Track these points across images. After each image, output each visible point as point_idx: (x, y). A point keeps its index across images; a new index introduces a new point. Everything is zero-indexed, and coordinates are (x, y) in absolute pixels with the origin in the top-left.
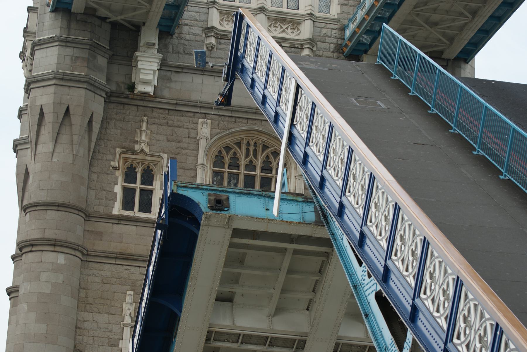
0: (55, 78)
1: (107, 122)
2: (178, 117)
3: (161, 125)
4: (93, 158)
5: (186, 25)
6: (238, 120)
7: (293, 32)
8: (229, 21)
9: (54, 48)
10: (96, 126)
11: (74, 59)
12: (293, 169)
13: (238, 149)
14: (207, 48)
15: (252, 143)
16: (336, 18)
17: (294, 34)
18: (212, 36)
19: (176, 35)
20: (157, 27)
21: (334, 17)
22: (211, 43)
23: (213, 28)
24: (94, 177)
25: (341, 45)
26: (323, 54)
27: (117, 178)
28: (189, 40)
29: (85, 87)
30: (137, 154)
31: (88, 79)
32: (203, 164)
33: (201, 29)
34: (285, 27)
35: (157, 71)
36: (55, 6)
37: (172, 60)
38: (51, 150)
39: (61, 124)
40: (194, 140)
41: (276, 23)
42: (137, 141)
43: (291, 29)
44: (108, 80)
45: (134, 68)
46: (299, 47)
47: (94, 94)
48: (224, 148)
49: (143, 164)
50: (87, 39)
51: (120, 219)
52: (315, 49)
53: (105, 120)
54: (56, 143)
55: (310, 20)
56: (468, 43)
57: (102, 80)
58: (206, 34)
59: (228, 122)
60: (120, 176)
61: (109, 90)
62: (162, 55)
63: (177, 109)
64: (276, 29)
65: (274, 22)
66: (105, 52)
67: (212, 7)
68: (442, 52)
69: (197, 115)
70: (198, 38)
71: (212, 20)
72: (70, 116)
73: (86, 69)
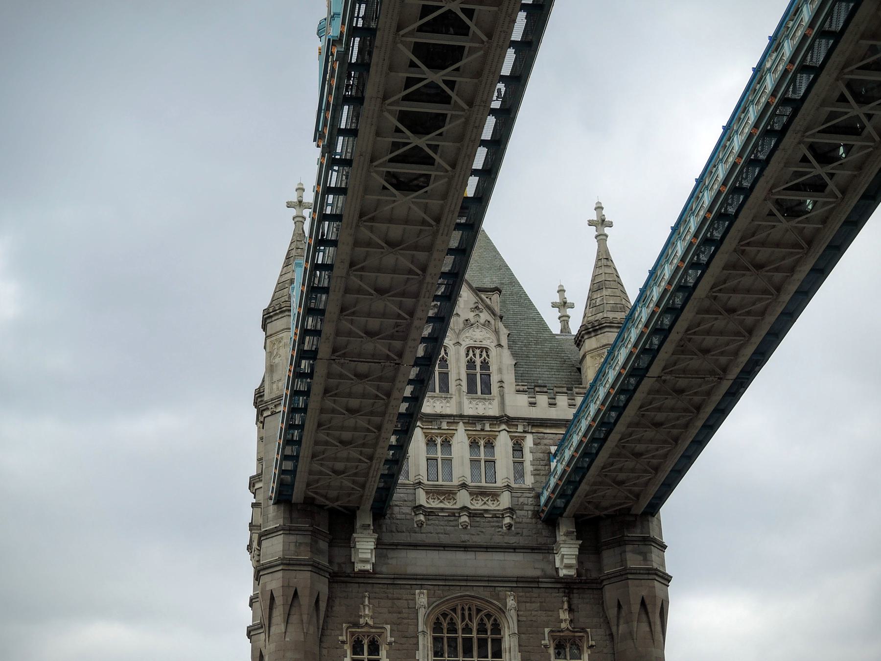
0: (282, 564)
1: (332, 600)
2: (396, 590)
3: (381, 599)
4: (322, 635)
5: (397, 506)
6: (452, 588)
7: (493, 504)
8: (434, 499)
9: (278, 537)
10: (323, 605)
11: (298, 545)
12: (506, 628)
13: (454, 615)
14: (417, 525)
15: (466, 608)
16: (531, 487)
17: (495, 505)
18: (421, 513)
19: (388, 515)
20: (370, 511)
21: (529, 487)
22: (420, 520)
23: (421, 506)
24: (325, 652)
25: (538, 511)
26: (522, 521)
27: (346, 651)
28: (400, 519)
29: (310, 569)
30: (362, 627)
31: (312, 562)
32: (423, 631)
33: (410, 508)
34: (485, 500)
35: (374, 550)
36: (277, 499)
37: (387, 538)
38: (283, 631)
39: (291, 605)
40: (414, 610)
41: (476, 497)
42: (361, 615)
43: (491, 501)
44: (330, 562)
45: (352, 549)
46: (501, 516)
47: (318, 575)
48: (441, 615)
49: (368, 636)
50: (308, 526)
52: (514, 517)
53: (331, 600)
54: (287, 623)
55: (507, 491)
56: (653, 498)
57: (324, 561)
58: (415, 512)
59: (443, 590)
60: (348, 648)
61: (331, 571)
62: (377, 535)
63: (395, 582)
64: (478, 502)
65: (475, 496)
66: (325, 537)
67: (418, 488)
68: (629, 509)
69: (413, 586)
70: (408, 517)
71: (419, 499)
72: (298, 598)
73: (310, 553)
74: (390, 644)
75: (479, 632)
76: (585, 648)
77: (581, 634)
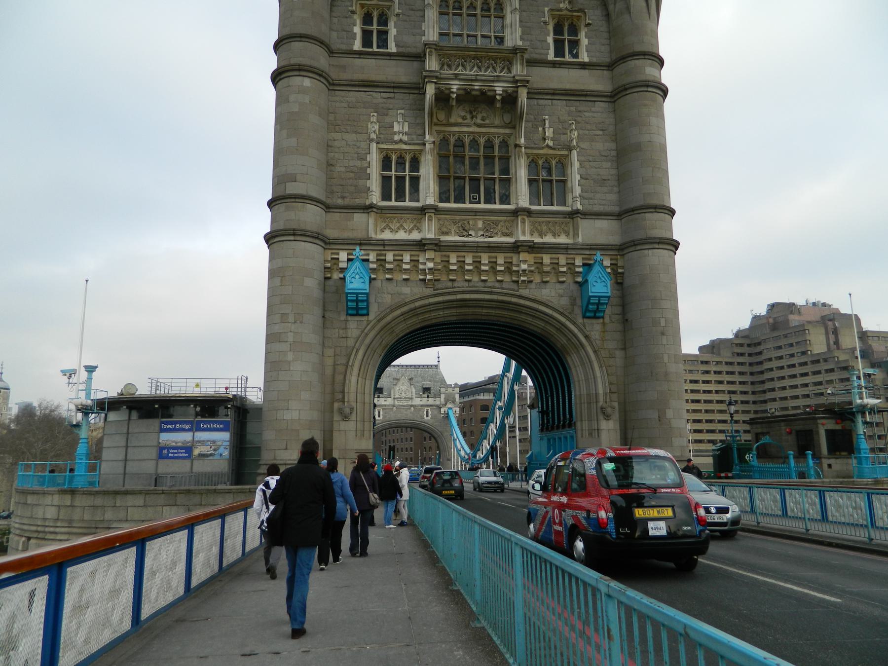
51: (360, 54)
60: (358, 19)
74: (398, 15)
75: (482, 10)
76: (582, 27)
77: (579, 14)
